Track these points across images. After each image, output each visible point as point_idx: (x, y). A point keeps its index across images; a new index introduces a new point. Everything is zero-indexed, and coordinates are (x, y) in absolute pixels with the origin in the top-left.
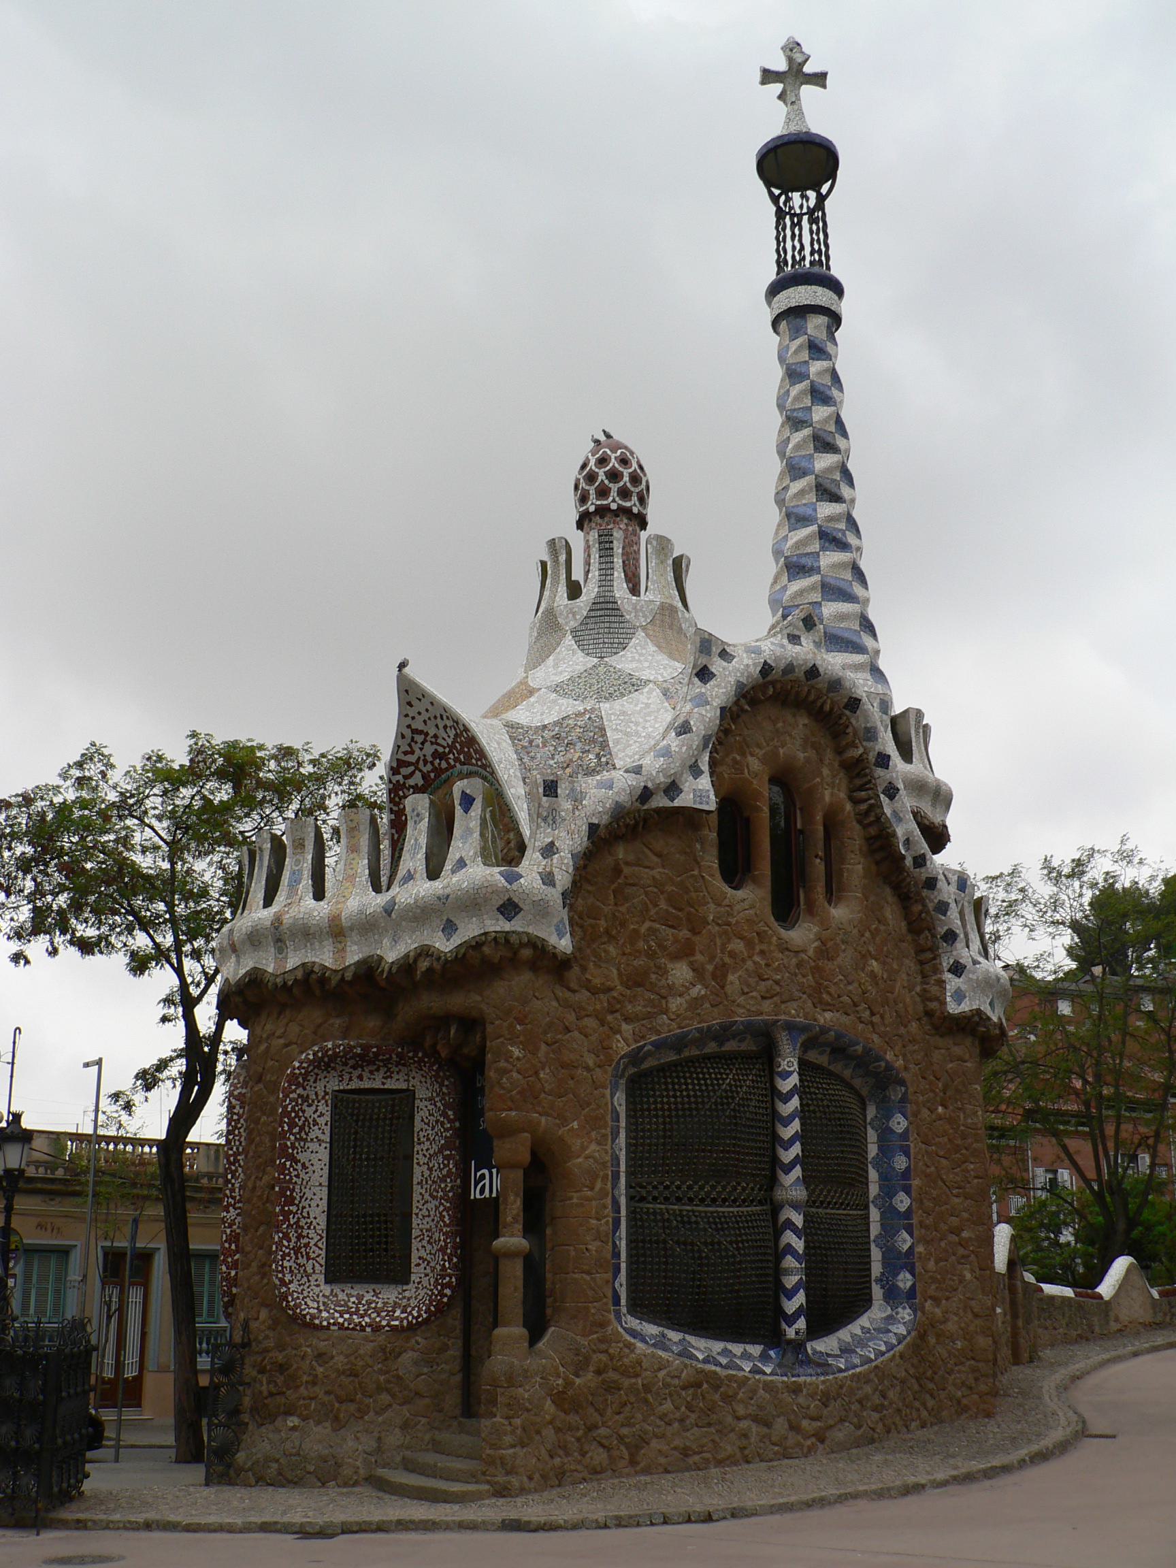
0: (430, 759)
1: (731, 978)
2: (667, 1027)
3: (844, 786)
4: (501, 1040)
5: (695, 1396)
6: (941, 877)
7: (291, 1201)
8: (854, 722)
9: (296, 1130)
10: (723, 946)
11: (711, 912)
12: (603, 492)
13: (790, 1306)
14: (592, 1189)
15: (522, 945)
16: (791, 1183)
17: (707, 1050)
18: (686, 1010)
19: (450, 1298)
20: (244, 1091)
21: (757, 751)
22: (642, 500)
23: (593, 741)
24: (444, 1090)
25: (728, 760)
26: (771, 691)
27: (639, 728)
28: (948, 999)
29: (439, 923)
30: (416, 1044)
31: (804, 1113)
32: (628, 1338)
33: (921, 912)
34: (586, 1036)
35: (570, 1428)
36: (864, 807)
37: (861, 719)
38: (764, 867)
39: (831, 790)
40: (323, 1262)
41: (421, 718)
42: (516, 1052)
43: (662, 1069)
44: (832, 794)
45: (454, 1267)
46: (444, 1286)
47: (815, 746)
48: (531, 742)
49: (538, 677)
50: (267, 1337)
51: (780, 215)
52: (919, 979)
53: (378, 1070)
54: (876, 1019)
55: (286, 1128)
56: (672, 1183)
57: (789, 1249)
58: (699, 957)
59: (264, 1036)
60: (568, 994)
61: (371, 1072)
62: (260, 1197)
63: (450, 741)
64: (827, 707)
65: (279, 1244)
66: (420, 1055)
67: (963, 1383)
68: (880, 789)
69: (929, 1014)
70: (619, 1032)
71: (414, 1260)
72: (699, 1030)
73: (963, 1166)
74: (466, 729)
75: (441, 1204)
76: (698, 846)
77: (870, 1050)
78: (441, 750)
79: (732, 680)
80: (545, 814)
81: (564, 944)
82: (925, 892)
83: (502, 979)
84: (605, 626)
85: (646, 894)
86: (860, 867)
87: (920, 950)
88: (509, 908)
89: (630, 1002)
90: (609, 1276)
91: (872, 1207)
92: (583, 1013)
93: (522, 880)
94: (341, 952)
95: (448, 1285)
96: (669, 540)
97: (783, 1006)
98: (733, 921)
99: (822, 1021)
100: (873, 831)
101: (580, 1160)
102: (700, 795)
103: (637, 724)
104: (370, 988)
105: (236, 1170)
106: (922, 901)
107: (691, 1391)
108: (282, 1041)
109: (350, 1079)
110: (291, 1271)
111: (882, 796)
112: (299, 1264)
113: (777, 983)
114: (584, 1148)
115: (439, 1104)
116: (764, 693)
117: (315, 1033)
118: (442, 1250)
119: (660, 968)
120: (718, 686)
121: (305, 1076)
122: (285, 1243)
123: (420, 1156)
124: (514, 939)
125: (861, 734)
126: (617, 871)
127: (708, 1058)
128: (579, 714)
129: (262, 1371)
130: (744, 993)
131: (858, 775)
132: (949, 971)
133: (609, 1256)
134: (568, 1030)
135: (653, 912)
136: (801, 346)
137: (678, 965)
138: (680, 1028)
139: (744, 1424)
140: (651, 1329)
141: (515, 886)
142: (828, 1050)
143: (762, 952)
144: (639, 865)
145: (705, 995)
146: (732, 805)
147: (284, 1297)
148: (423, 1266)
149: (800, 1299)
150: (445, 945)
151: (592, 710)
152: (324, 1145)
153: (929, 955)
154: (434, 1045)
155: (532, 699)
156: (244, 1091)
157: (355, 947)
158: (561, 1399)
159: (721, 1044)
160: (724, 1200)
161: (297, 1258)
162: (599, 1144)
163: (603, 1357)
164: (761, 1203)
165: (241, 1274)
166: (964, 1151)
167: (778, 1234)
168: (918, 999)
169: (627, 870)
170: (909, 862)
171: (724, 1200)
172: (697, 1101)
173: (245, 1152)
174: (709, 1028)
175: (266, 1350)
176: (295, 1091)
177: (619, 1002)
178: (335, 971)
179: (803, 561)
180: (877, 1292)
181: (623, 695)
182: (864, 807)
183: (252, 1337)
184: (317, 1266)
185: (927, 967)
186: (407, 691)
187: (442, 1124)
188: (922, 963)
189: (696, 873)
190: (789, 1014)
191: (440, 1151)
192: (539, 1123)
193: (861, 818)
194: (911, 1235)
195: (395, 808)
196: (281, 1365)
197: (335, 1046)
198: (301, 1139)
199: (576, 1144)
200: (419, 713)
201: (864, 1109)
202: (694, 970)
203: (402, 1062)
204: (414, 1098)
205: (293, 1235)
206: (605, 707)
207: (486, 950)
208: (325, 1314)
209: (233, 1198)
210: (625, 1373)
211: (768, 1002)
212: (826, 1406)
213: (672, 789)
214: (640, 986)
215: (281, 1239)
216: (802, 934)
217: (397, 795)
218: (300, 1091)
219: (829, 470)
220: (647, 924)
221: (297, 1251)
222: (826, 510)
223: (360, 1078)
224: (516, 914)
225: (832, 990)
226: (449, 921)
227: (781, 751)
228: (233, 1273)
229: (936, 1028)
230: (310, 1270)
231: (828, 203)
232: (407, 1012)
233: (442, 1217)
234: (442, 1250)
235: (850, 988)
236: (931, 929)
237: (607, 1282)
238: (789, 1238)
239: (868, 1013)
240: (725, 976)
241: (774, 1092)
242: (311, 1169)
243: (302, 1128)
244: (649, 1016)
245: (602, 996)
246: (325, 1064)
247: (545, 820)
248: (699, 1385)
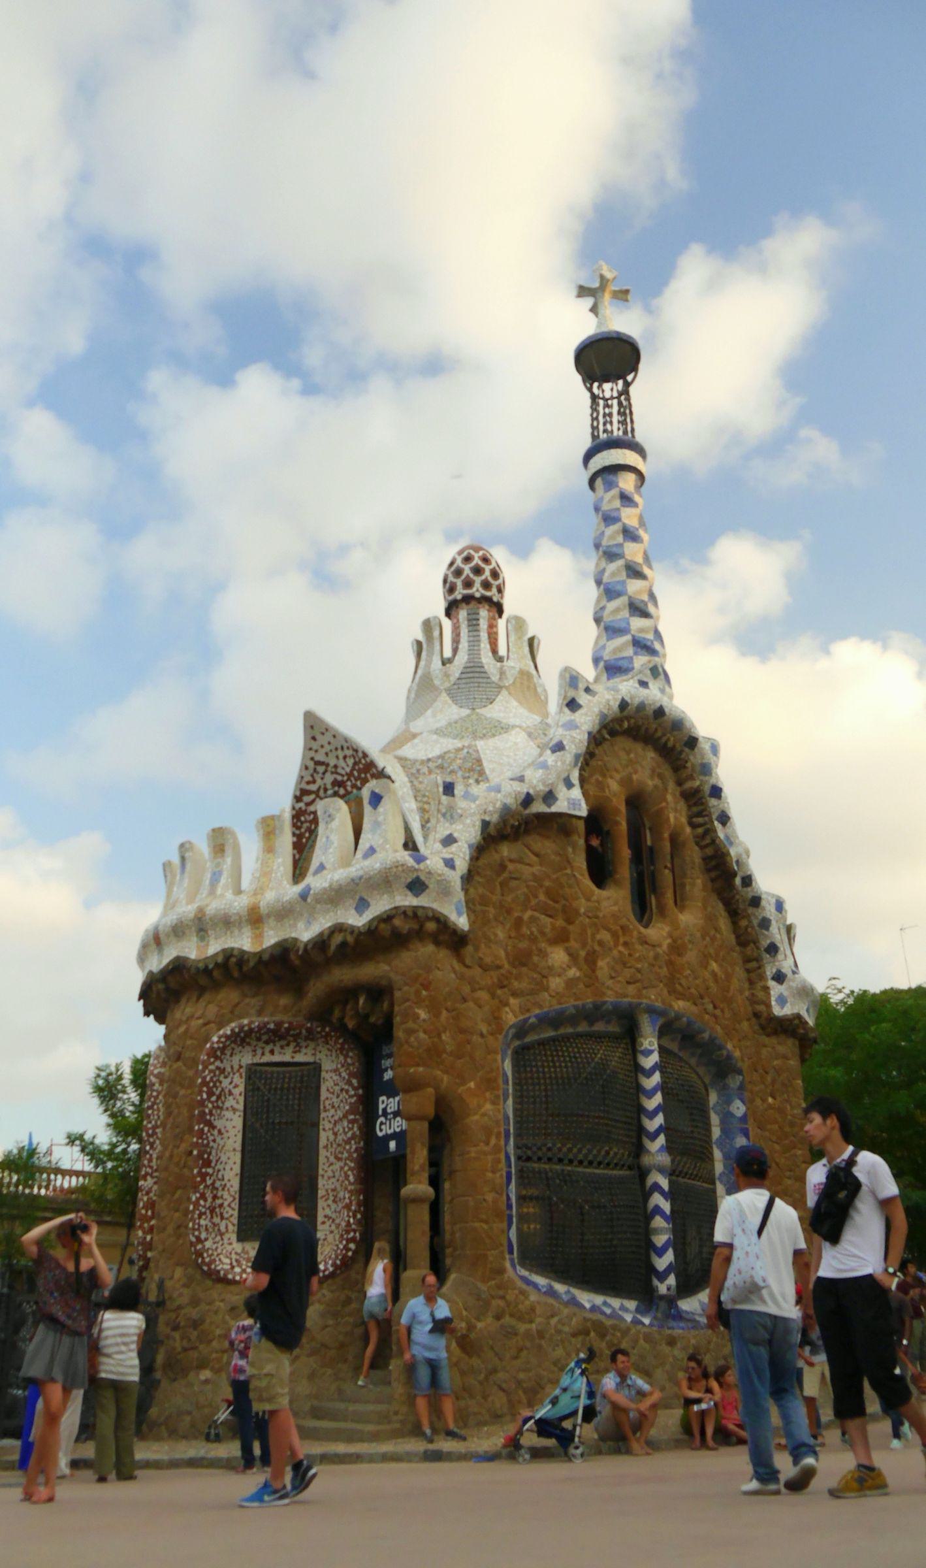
0: (329, 786)
1: (600, 963)
2: (548, 1003)
3: (684, 813)
4: (408, 1004)
6: (763, 896)
7: (208, 1163)
8: (691, 757)
9: (214, 1098)
10: (593, 935)
11: (582, 906)
12: (468, 584)
13: (663, 1262)
15: (428, 919)
19: (355, 1252)
20: (163, 1070)
22: (500, 590)
23: (471, 770)
24: (349, 1060)
25: (593, 780)
26: (626, 725)
27: (511, 761)
28: (773, 1003)
29: (351, 903)
30: (325, 1020)
31: (663, 1087)
32: (524, 1286)
33: (747, 927)
34: (480, 1007)
36: (700, 830)
37: (698, 757)
38: (624, 870)
39: (676, 815)
40: (236, 1222)
41: (323, 751)
42: (423, 1014)
43: (542, 1043)
44: (676, 818)
45: (358, 1222)
46: (349, 1241)
47: (660, 776)
48: (418, 771)
49: (417, 726)
50: (181, 1295)
51: (594, 398)
52: (747, 985)
53: (288, 1045)
54: (718, 1012)
55: (205, 1096)
56: (554, 1145)
57: (658, 1210)
58: (573, 944)
59: (184, 1018)
61: (282, 1047)
62: (177, 1164)
63: (348, 770)
64: (670, 744)
65: (197, 1204)
66: (327, 1029)
68: (714, 817)
69: (757, 1015)
70: (507, 1004)
71: (320, 1219)
72: (575, 1007)
73: (793, 1152)
74: (365, 755)
75: (346, 1164)
76: (570, 850)
78: (339, 778)
79: (596, 710)
80: (444, 810)
81: (462, 922)
82: (751, 910)
83: (408, 950)
84: (474, 684)
85: (528, 887)
86: (699, 881)
87: (747, 960)
88: (417, 886)
89: (516, 979)
90: (505, 1225)
91: (718, 1183)
93: (428, 862)
94: (259, 937)
95: (353, 1240)
96: (524, 621)
97: (644, 992)
98: (601, 915)
100: (709, 851)
102: (573, 803)
103: (508, 756)
104: (282, 968)
105: (154, 1142)
106: (748, 917)
107: (580, 1338)
108: (201, 1021)
109: (263, 1054)
110: (207, 1229)
111: (716, 823)
112: (214, 1225)
113: (639, 971)
114: (479, 1107)
115: (344, 1074)
116: (621, 726)
117: (232, 1012)
118: (348, 1207)
119: (540, 950)
120: (586, 714)
121: (223, 1050)
122: (202, 1202)
123: (326, 1122)
124: (420, 913)
125: (698, 769)
126: (503, 867)
127: (580, 1035)
128: (459, 750)
129: (176, 1328)
130: (612, 978)
131: (695, 804)
132: (773, 978)
133: (504, 1207)
134: (465, 1000)
135: (534, 902)
136: (613, 497)
140: (541, 1281)
141: (422, 866)
142: (679, 1036)
143: (626, 944)
146: (596, 822)
147: (199, 1254)
148: (328, 1223)
149: (669, 1257)
150: (358, 920)
151: (469, 747)
152: (238, 1114)
153: (754, 964)
154: (341, 1019)
155: (416, 741)
156: (163, 1070)
157: (271, 933)
159: (591, 1024)
160: (600, 1163)
162: (493, 1103)
163: (501, 1303)
164: (630, 1168)
165: (156, 1238)
167: (647, 1196)
168: (747, 1003)
169: (511, 866)
170: (738, 881)
171: (600, 1163)
172: (574, 1074)
173: (163, 1125)
174: (584, 1006)
175: (179, 1308)
176: (213, 1063)
177: (507, 978)
178: (255, 954)
179: (620, 663)
181: (494, 735)
182: (700, 830)
183: (166, 1296)
184: (231, 1227)
185: (753, 975)
186: (312, 727)
187: (347, 1092)
188: (748, 971)
189: (569, 871)
191: (345, 1116)
192: (442, 1080)
193: (699, 840)
195: (297, 832)
196: (195, 1321)
197: (251, 1022)
198: (218, 1107)
199: (473, 1102)
200: (322, 746)
201: (708, 1095)
202: (570, 954)
203: (311, 1036)
204: (320, 1071)
205: (209, 1195)
206: (480, 744)
207: (397, 922)
208: (237, 1270)
209: (151, 1167)
210: (520, 1319)
213: (549, 797)
214: (524, 965)
215: (198, 1199)
216: (658, 932)
217: (299, 820)
218: (218, 1063)
219: (640, 592)
220: (529, 913)
221: (212, 1210)
222: (637, 623)
223: (272, 1052)
224: (423, 891)
225: (683, 981)
226: (362, 899)
228: (148, 1238)
229: (763, 1028)
230: (223, 1229)
231: (632, 389)
232: (317, 988)
233: (347, 1177)
234: (348, 1207)
236: (756, 942)
238: (657, 1200)
241: (638, 1069)
242: (226, 1135)
243: (219, 1097)
244: (533, 993)
245: (492, 973)
246: (241, 1039)
247: (444, 815)
248: (587, 1333)
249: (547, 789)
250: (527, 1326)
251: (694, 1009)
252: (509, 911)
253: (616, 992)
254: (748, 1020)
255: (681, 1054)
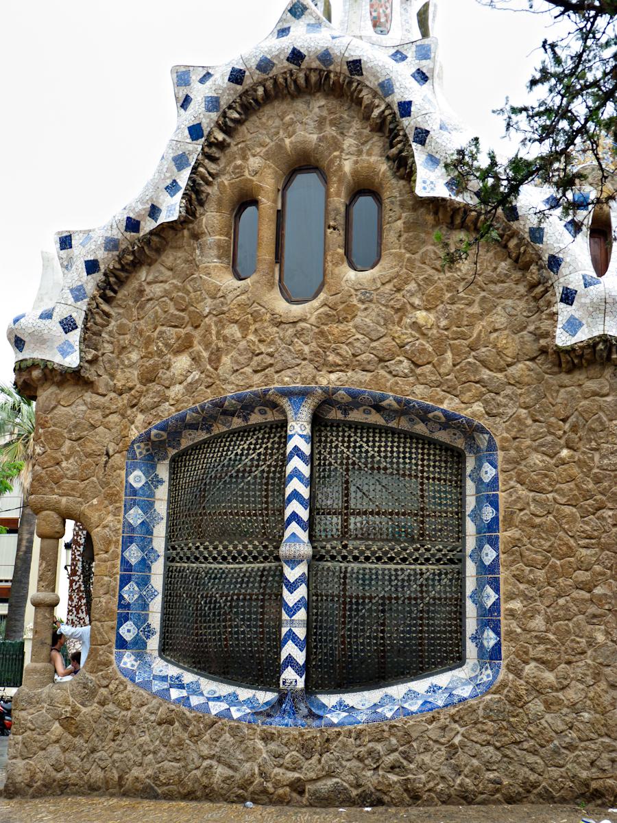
2: (167, 411)
3: (377, 150)
5: (166, 732)
8: (368, 83)
11: (206, 306)
14: (107, 552)
16: (296, 541)
17: (234, 426)
18: (183, 395)
21: (258, 150)
25: (230, 169)
33: (518, 246)
35: (75, 748)
37: (371, 78)
44: (356, 162)
47: (333, 124)
58: (198, 347)
60: (96, 398)
67: (592, 763)
68: (411, 139)
69: (543, 351)
70: (133, 423)
76: (198, 252)
77: (408, 402)
80: (65, 263)
82: (514, 225)
92: (108, 412)
97: (276, 376)
98: (225, 309)
99: (324, 382)
101: (99, 529)
107: (165, 726)
113: (271, 355)
119: (164, 363)
126: (141, 292)
134: (93, 427)
137: (179, 358)
138: (177, 411)
139: (206, 763)
144: (156, 282)
145: (199, 379)
153: (540, 289)
158: (69, 723)
159: (246, 419)
161: (78, 613)
163: (104, 691)
166: (599, 497)
168: (528, 338)
169: (148, 289)
174: (202, 408)
180: (471, 649)
185: (541, 303)
188: (536, 299)
190: (282, 382)
194: (497, 590)
202: (193, 359)
211: (259, 374)
212: (307, 759)
213: (154, 211)
227: (287, 141)
235: (374, 344)
237: (113, 628)
239: (406, 363)
240: (219, 360)
248: (171, 723)
249: (148, 206)
250: (124, 713)
251: (367, 377)
252: (141, 335)
253: (237, 385)
254: (533, 359)
255: (393, 424)
